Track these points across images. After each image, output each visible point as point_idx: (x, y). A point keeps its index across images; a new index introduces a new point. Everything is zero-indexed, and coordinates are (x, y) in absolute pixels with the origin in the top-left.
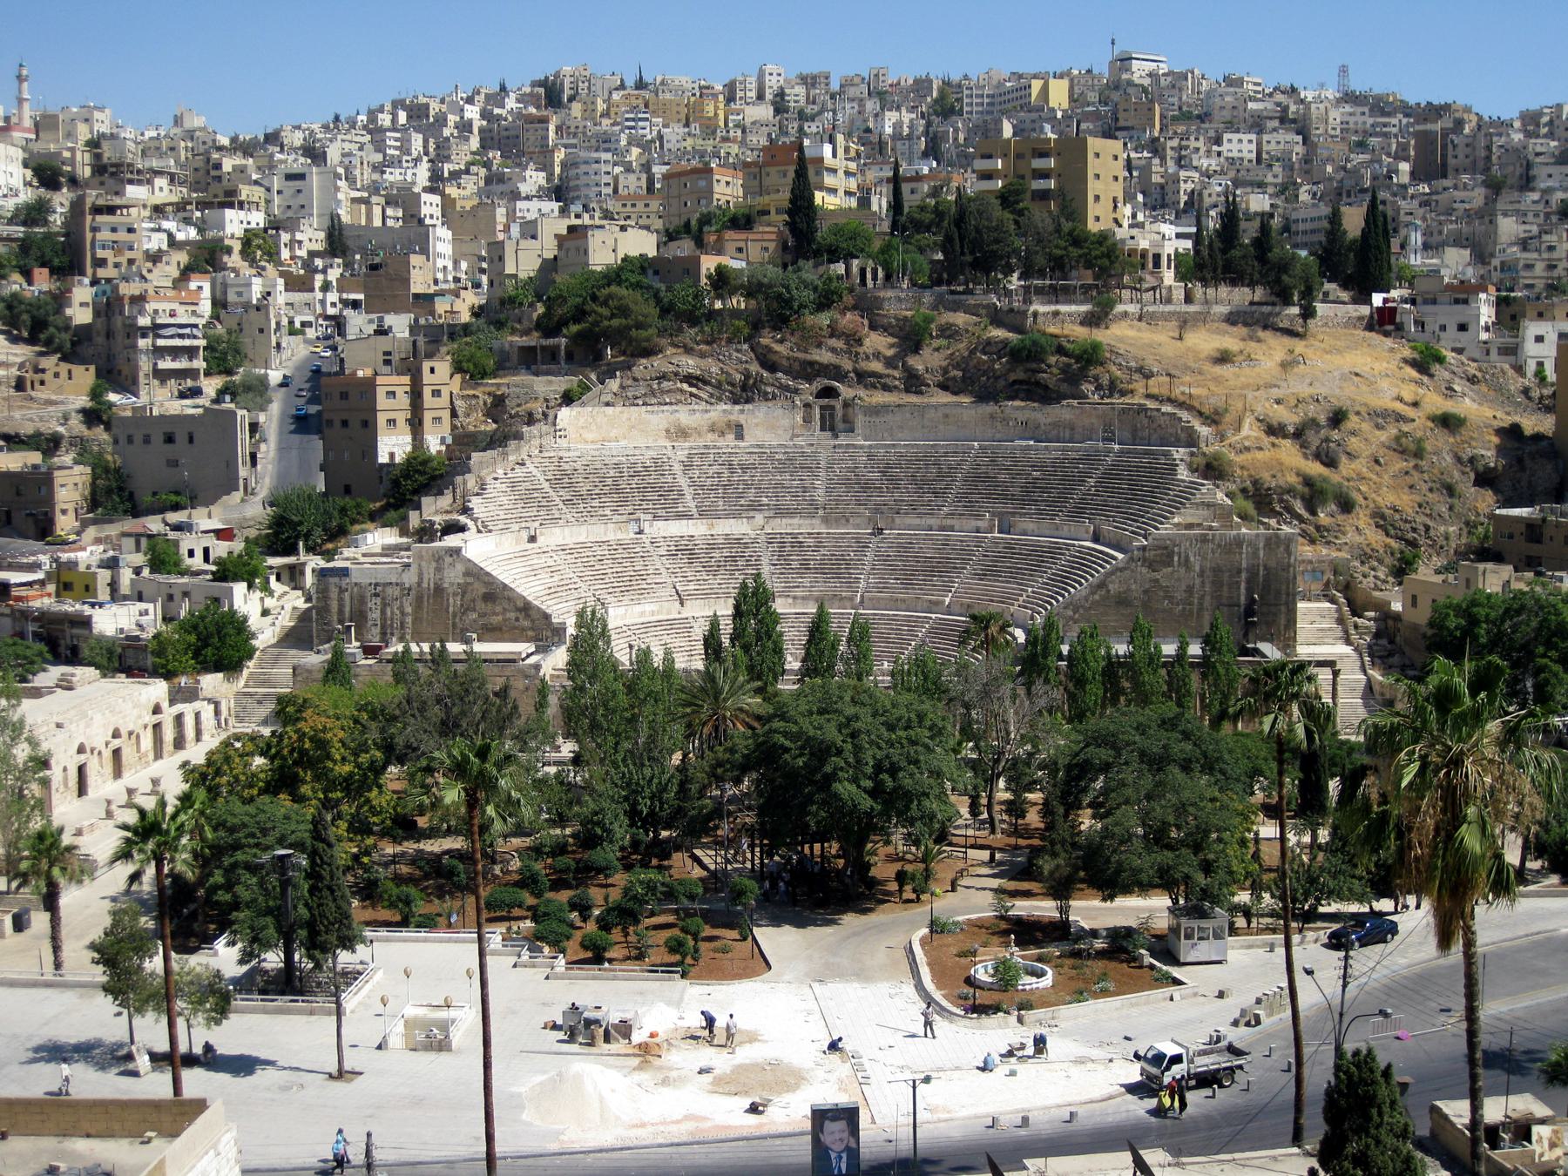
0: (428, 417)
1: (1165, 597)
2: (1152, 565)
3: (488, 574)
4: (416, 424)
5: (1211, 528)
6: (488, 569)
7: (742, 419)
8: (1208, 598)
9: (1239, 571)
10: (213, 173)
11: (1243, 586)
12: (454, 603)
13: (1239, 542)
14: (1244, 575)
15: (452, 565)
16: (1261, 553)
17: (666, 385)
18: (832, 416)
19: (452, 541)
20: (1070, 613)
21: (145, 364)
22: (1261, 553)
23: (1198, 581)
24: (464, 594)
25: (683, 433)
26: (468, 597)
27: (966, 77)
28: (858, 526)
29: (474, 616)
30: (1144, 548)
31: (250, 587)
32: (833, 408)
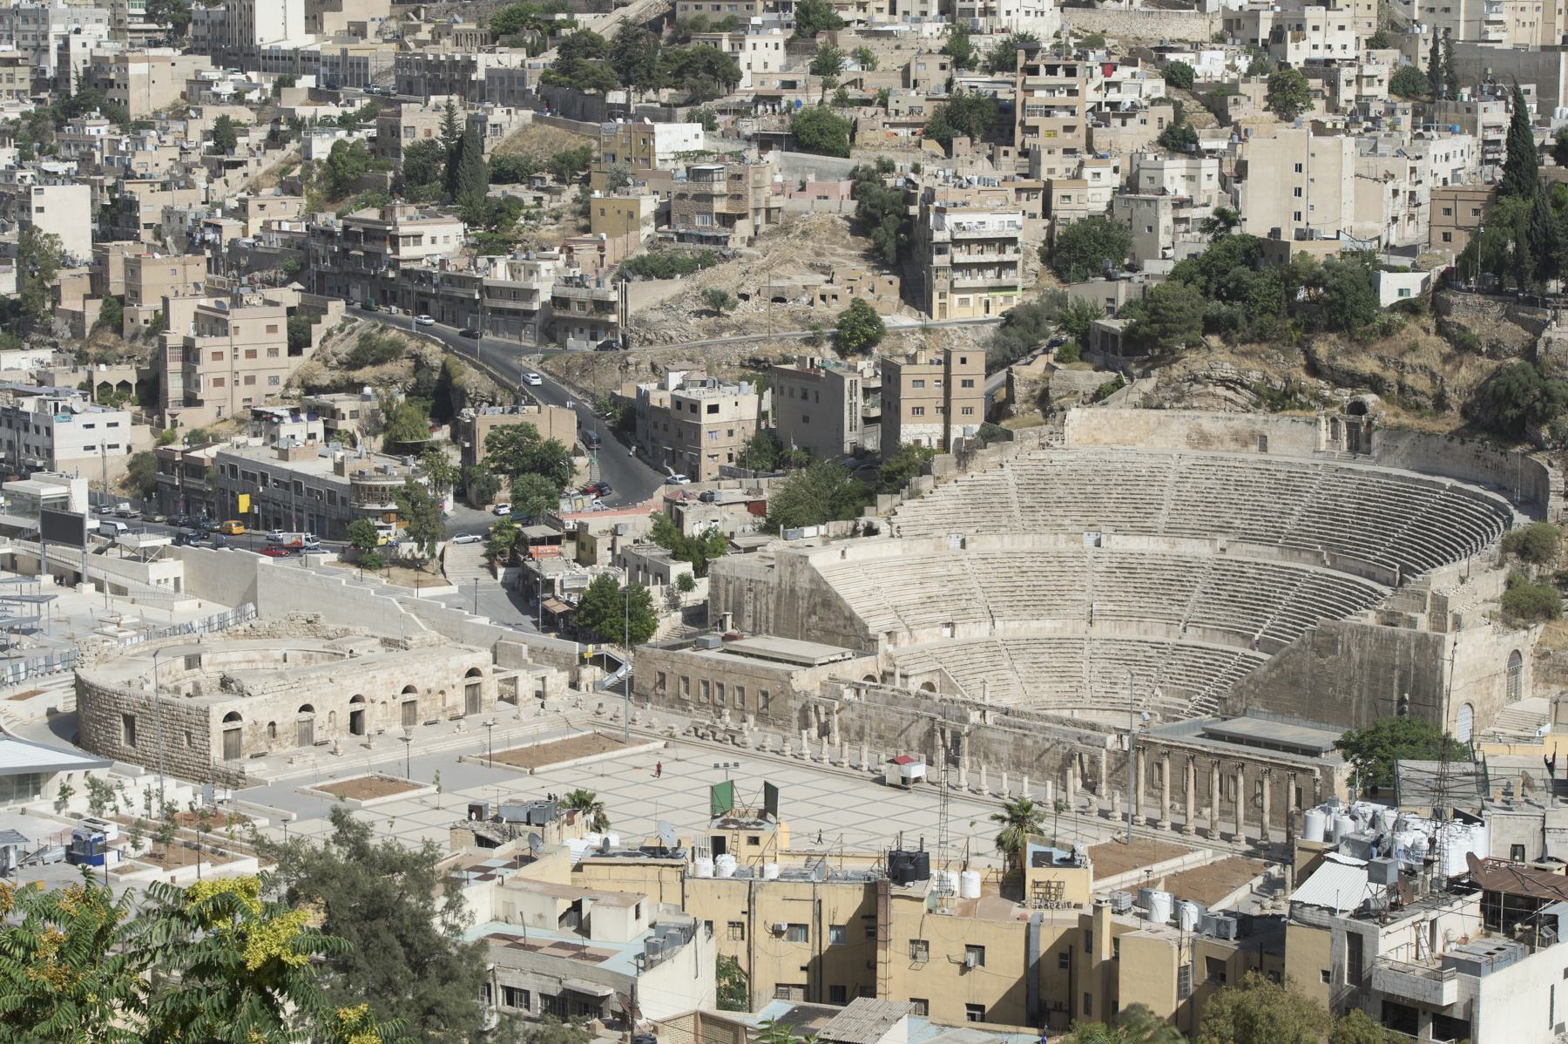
0: (956, 408)
6: (828, 580)
8: (1365, 690)
11: (1396, 682)
14: (1397, 673)
15: (802, 571)
17: (1197, 388)
18: (1358, 432)
21: (940, 283)
25: (1203, 439)
28: (1307, 561)
29: (814, 619)
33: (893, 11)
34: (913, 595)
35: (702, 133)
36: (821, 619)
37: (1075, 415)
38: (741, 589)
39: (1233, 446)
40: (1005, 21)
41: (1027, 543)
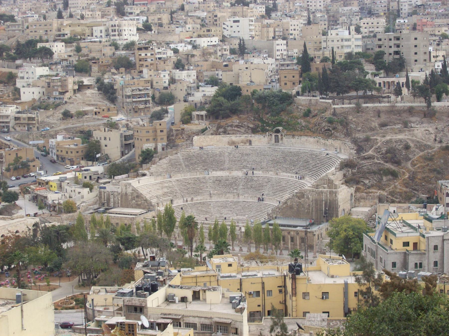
0: (159, 138)
1: (303, 207)
2: (299, 198)
4: (155, 140)
7: (251, 138)
8: (314, 208)
9: (323, 201)
10: (215, 18)
11: (323, 205)
12: (130, 197)
13: (322, 192)
14: (324, 202)
17: (229, 128)
18: (278, 138)
20: (278, 210)
24: (132, 195)
29: (134, 201)
30: (297, 193)
33: (92, 36)
34: (160, 192)
35: (48, 70)
36: (136, 201)
37: (195, 138)
38: (109, 195)
40: (126, 37)
41: (188, 176)
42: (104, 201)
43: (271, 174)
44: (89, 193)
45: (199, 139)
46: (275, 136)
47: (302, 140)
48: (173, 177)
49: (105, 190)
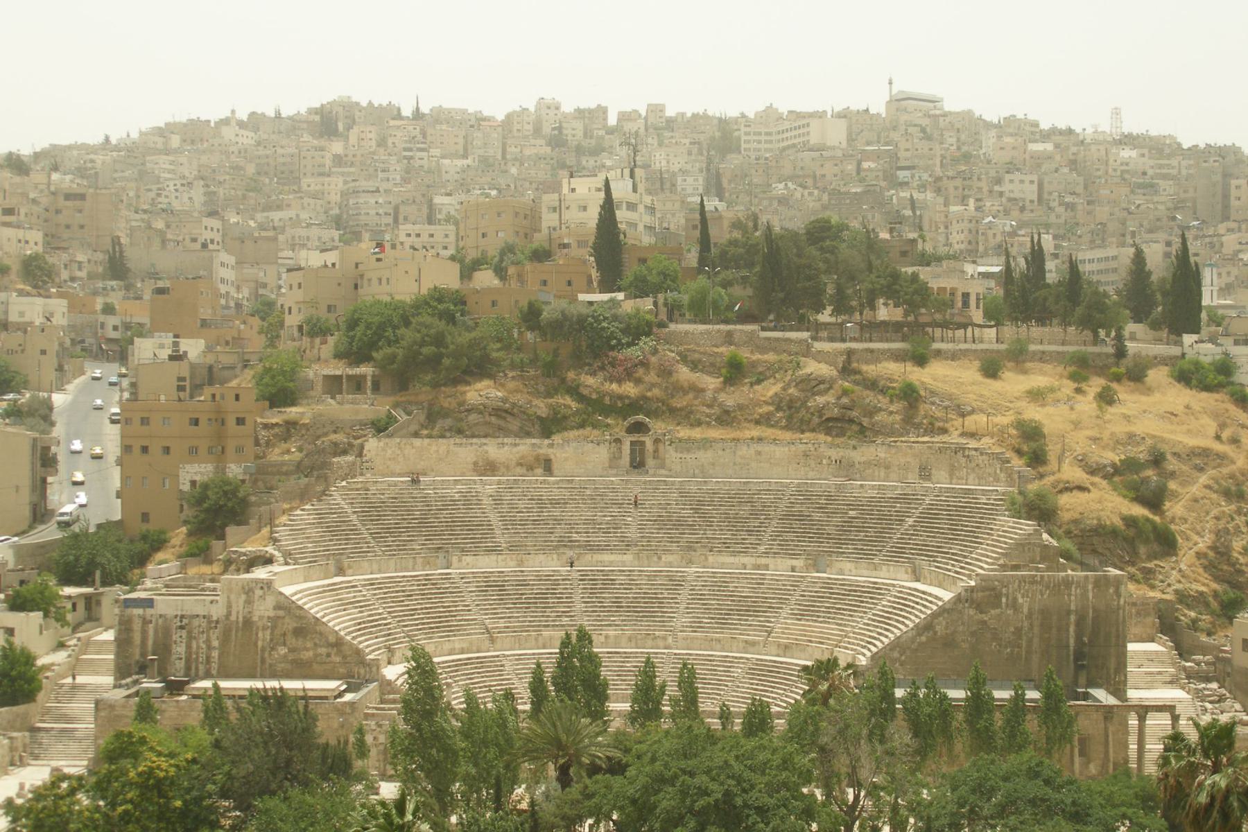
0: (231, 446)
2: (979, 607)
3: (300, 608)
5: (1038, 569)
8: (1036, 640)
9: (1069, 613)
11: (1072, 629)
12: (264, 637)
13: (1068, 583)
14: (1073, 618)
15: (262, 597)
16: (1091, 595)
18: (642, 452)
19: (260, 573)
20: (896, 655)
22: (1091, 595)
23: (1026, 624)
24: (274, 628)
25: (490, 468)
26: (278, 632)
27: (743, 116)
29: (283, 651)
30: (972, 589)
31: (46, 615)
32: (643, 443)
36: (292, 650)
38: (167, 632)
39: (519, 470)
42: (144, 655)
43: (670, 563)
44: (41, 633)
45: (383, 450)
46: (632, 443)
47: (739, 453)
48: (350, 571)
49: (149, 611)
